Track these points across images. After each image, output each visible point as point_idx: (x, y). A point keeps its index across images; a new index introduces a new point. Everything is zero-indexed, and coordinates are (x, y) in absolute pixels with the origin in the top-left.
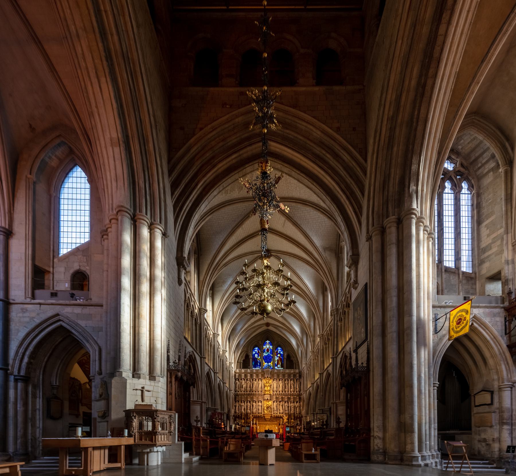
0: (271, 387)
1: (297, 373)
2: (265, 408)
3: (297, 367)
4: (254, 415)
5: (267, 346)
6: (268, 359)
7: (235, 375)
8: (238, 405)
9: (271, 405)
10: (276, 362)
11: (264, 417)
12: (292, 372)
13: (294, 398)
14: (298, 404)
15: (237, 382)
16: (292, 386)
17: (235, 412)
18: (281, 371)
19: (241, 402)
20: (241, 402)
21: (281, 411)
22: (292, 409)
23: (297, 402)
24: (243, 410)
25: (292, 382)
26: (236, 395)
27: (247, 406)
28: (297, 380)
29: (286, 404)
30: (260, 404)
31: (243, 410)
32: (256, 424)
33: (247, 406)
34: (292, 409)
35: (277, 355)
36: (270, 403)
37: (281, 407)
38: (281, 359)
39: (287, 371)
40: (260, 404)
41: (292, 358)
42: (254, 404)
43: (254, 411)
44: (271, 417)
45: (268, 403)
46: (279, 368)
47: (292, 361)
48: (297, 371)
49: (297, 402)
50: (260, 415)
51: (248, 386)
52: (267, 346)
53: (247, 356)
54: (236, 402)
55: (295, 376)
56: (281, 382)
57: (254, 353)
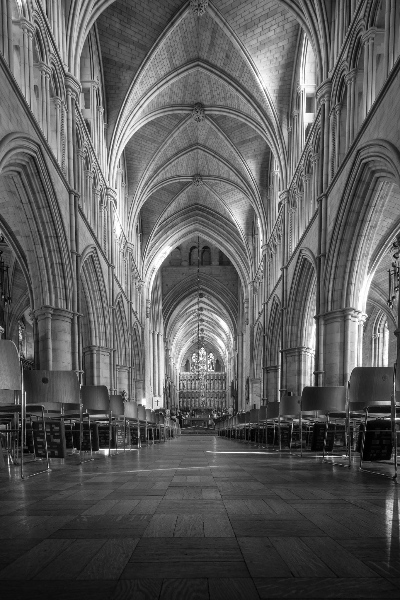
0: (204, 385)
1: (223, 375)
2: (201, 403)
3: (223, 370)
4: (193, 408)
5: (202, 352)
6: (204, 363)
7: (180, 377)
8: (181, 401)
9: (205, 401)
10: (209, 366)
11: (200, 409)
12: (220, 374)
13: (221, 394)
14: (224, 399)
15: (181, 382)
16: (220, 386)
17: (180, 407)
18: (212, 373)
19: (184, 398)
20: (184, 398)
21: (212, 405)
22: (220, 403)
23: (223, 398)
24: (185, 405)
25: (220, 382)
26: (180, 393)
27: (188, 402)
28: (223, 380)
29: (216, 400)
30: (197, 400)
31: (185, 405)
32: (194, 415)
33: (188, 402)
34: (220, 403)
35: (209, 360)
36: (203, 399)
37: (212, 402)
38: (212, 363)
39: (216, 373)
40: (197, 400)
41: (220, 363)
42: (193, 400)
43: (193, 405)
44: (205, 409)
45: (202, 399)
46: (210, 370)
47: (220, 365)
48: (223, 373)
49: (223, 398)
50: (197, 408)
51: (189, 386)
52: (202, 352)
53: (188, 361)
54: (180, 398)
55: (222, 377)
56: (212, 382)
57: (193, 358)
